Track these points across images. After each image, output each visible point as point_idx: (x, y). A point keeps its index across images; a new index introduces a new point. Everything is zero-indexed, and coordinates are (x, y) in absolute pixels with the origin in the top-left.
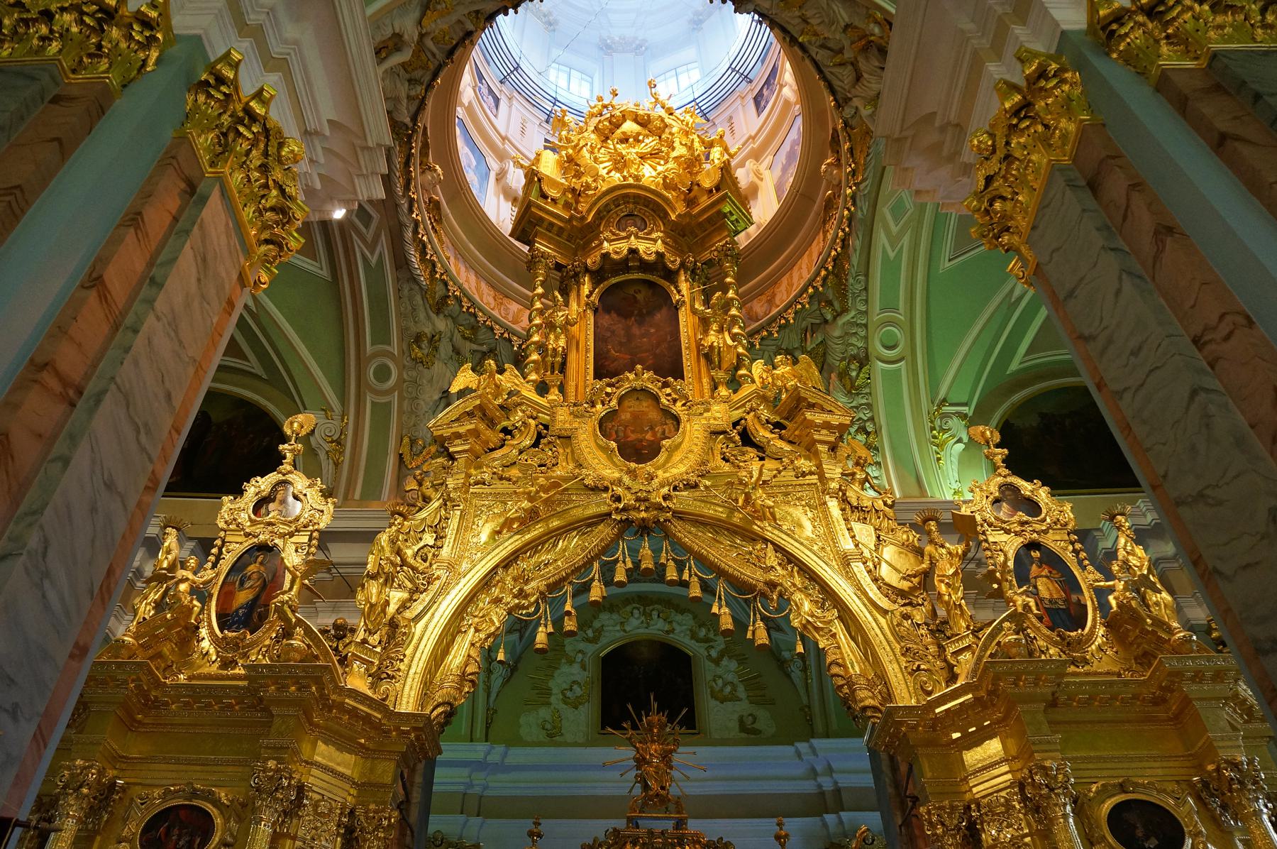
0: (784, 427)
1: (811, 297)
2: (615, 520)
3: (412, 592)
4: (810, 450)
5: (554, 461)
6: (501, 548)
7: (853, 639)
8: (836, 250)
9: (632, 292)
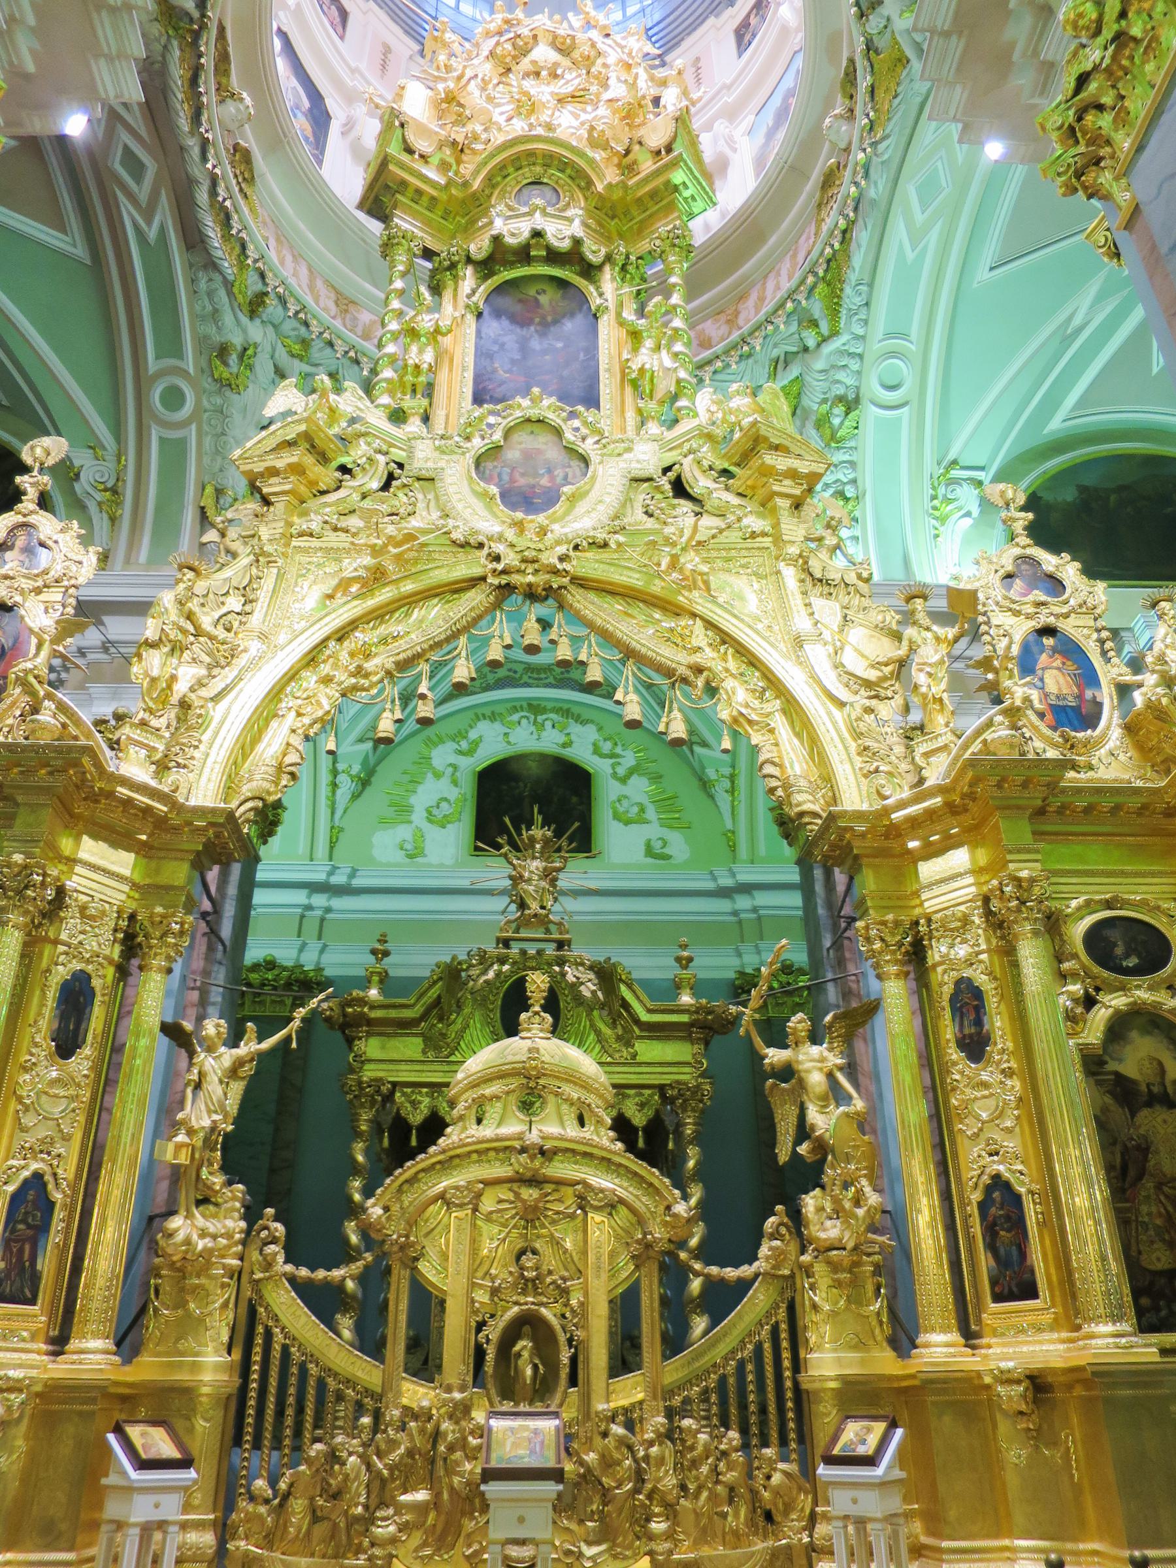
3: (210, 667)
4: (766, 504)
6: (333, 616)
7: (798, 735)
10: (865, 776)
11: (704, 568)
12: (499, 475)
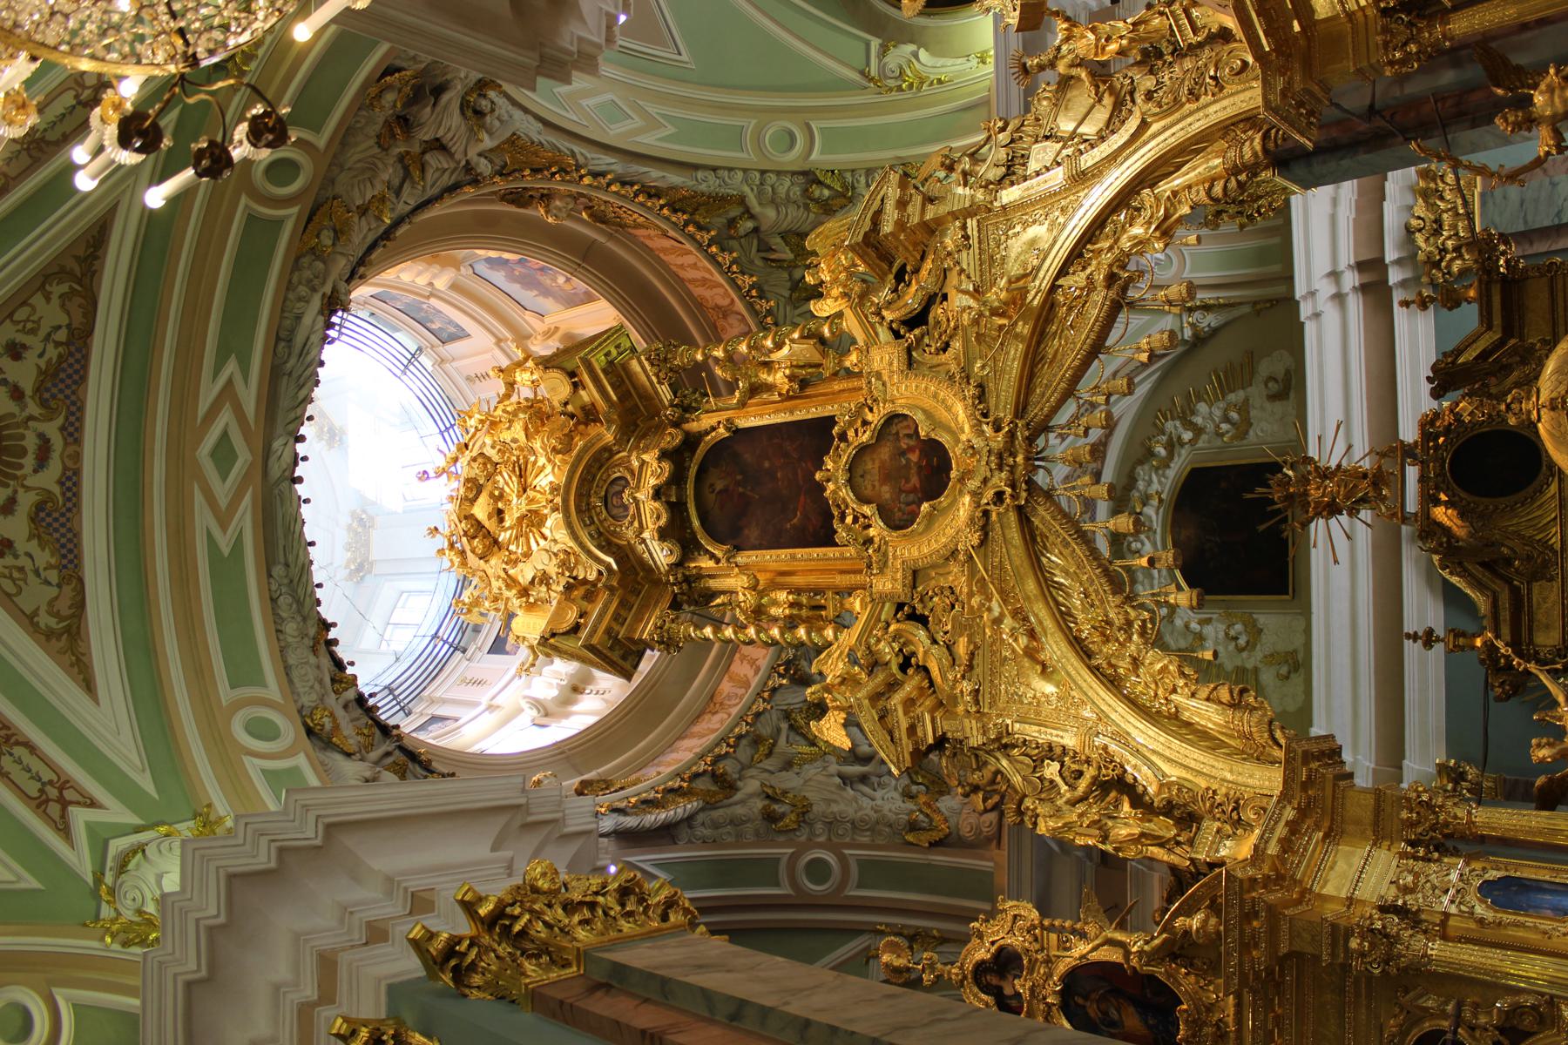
0: (902, 271)
1: (723, 250)
2: (1027, 500)
4: (932, 229)
5: (947, 593)
8: (662, 207)
9: (713, 496)
10: (1222, 89)
11: (1003, 283)
12: (908, 504)
